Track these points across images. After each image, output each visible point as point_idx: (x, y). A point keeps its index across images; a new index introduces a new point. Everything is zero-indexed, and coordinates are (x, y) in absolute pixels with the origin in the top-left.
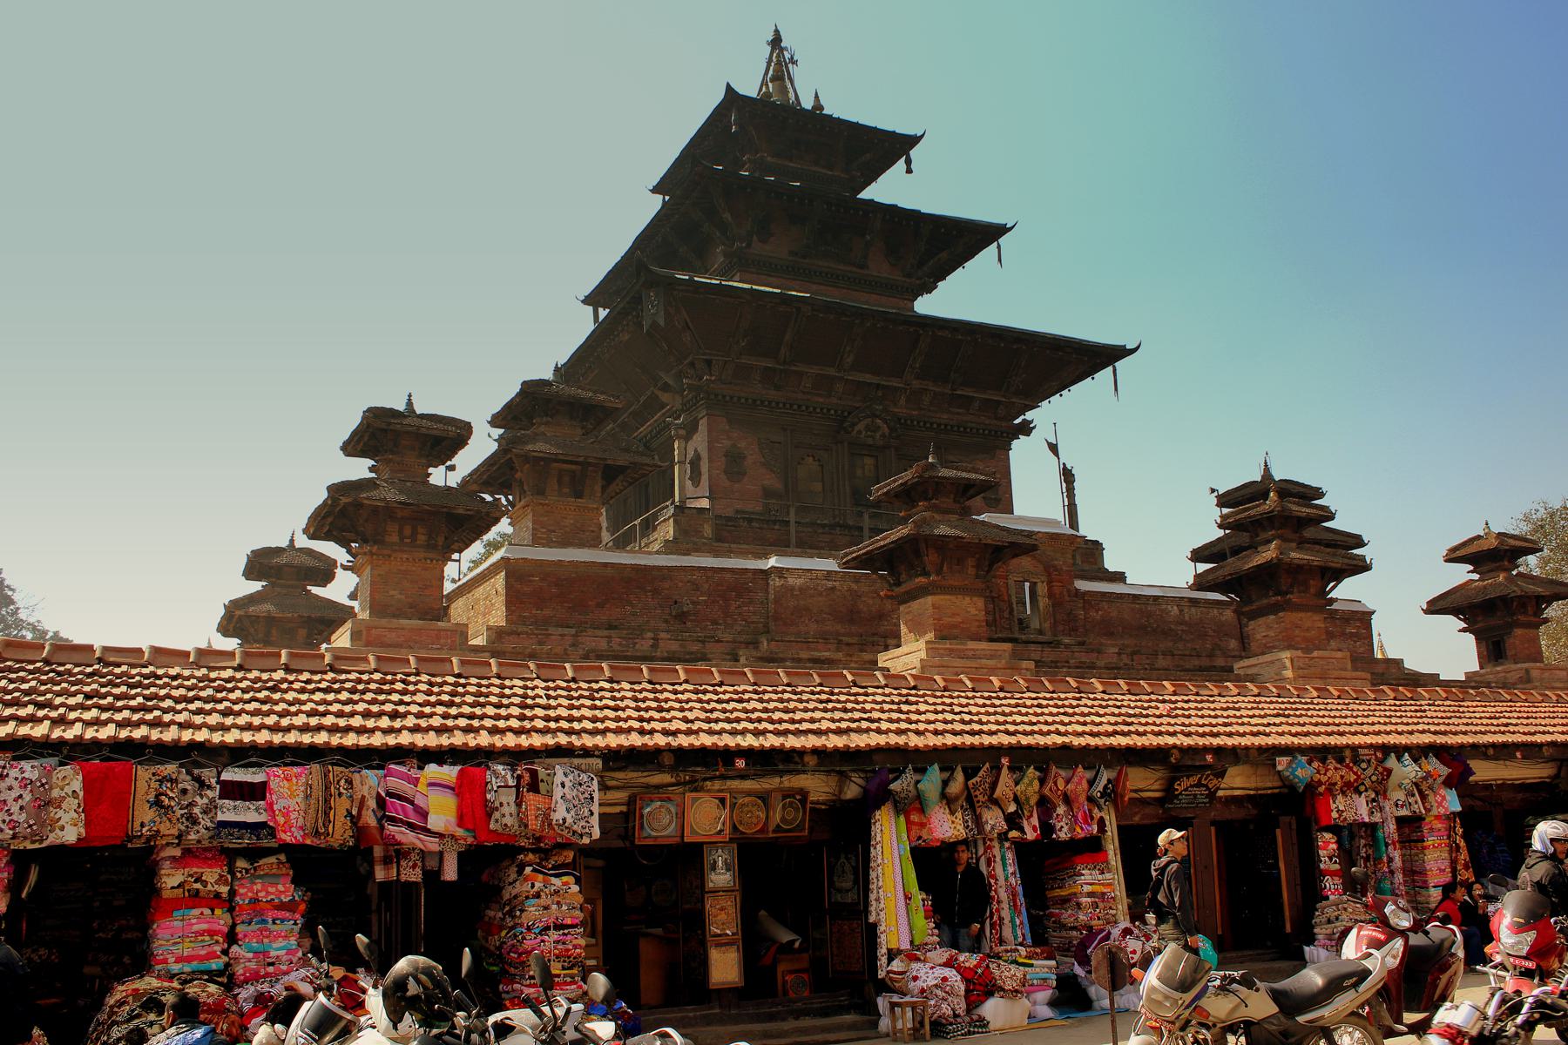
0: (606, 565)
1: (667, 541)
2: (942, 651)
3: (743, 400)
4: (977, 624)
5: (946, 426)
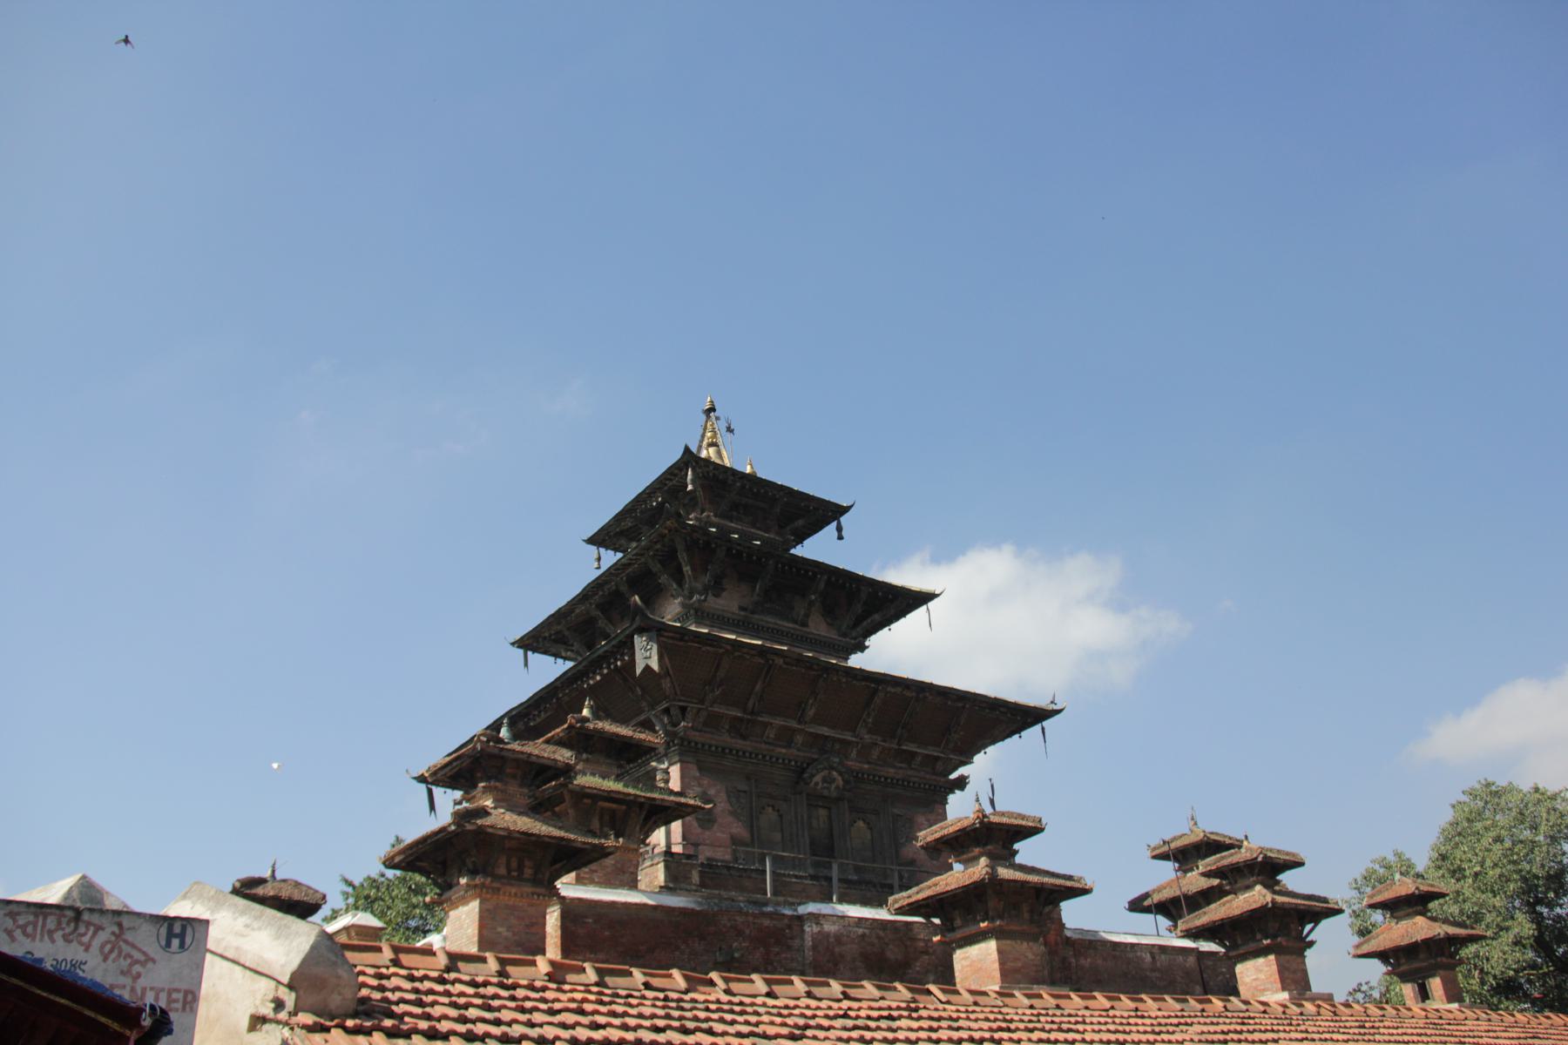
1: (661, 887)
3: (713, 748)
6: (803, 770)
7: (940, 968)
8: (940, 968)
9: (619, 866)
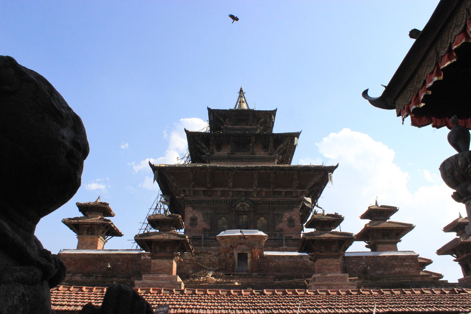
0: (89, 254)
2: (148, 278)
3: (196, 201)
4: (169, 269)
5: (272, 202)
6: (233, 203)
7: (196, 269)
8: (196, 269)
9: (91, 243)
